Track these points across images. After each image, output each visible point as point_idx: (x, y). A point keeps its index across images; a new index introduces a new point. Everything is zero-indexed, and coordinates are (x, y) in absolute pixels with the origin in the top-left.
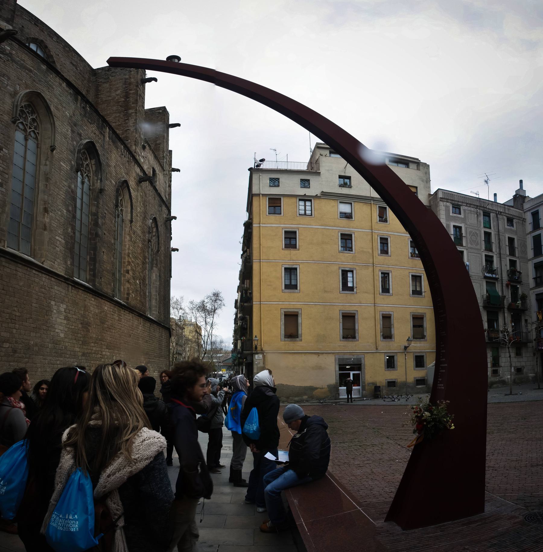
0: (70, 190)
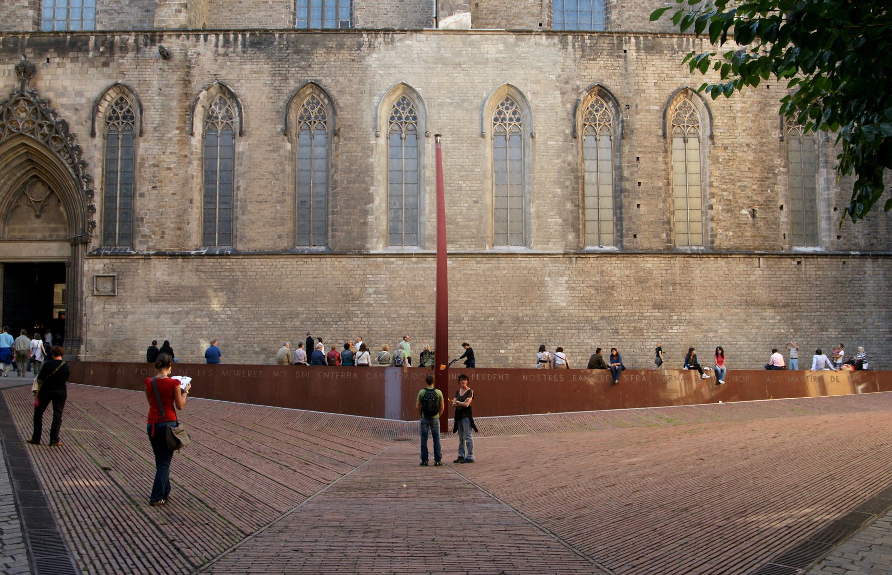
0: (566, 165)
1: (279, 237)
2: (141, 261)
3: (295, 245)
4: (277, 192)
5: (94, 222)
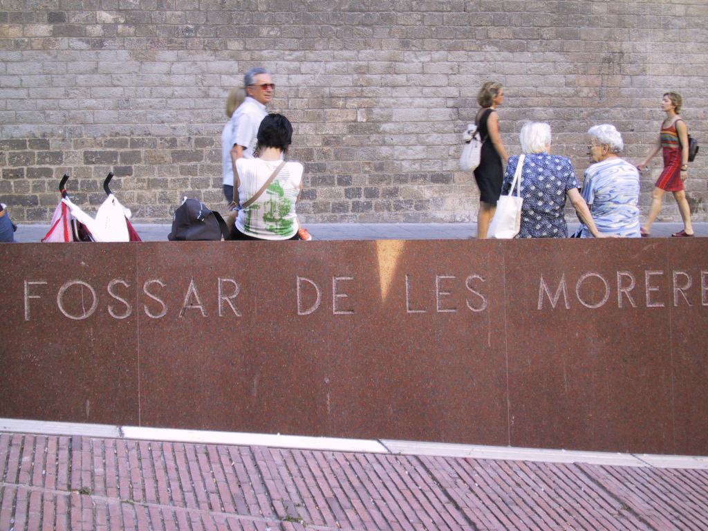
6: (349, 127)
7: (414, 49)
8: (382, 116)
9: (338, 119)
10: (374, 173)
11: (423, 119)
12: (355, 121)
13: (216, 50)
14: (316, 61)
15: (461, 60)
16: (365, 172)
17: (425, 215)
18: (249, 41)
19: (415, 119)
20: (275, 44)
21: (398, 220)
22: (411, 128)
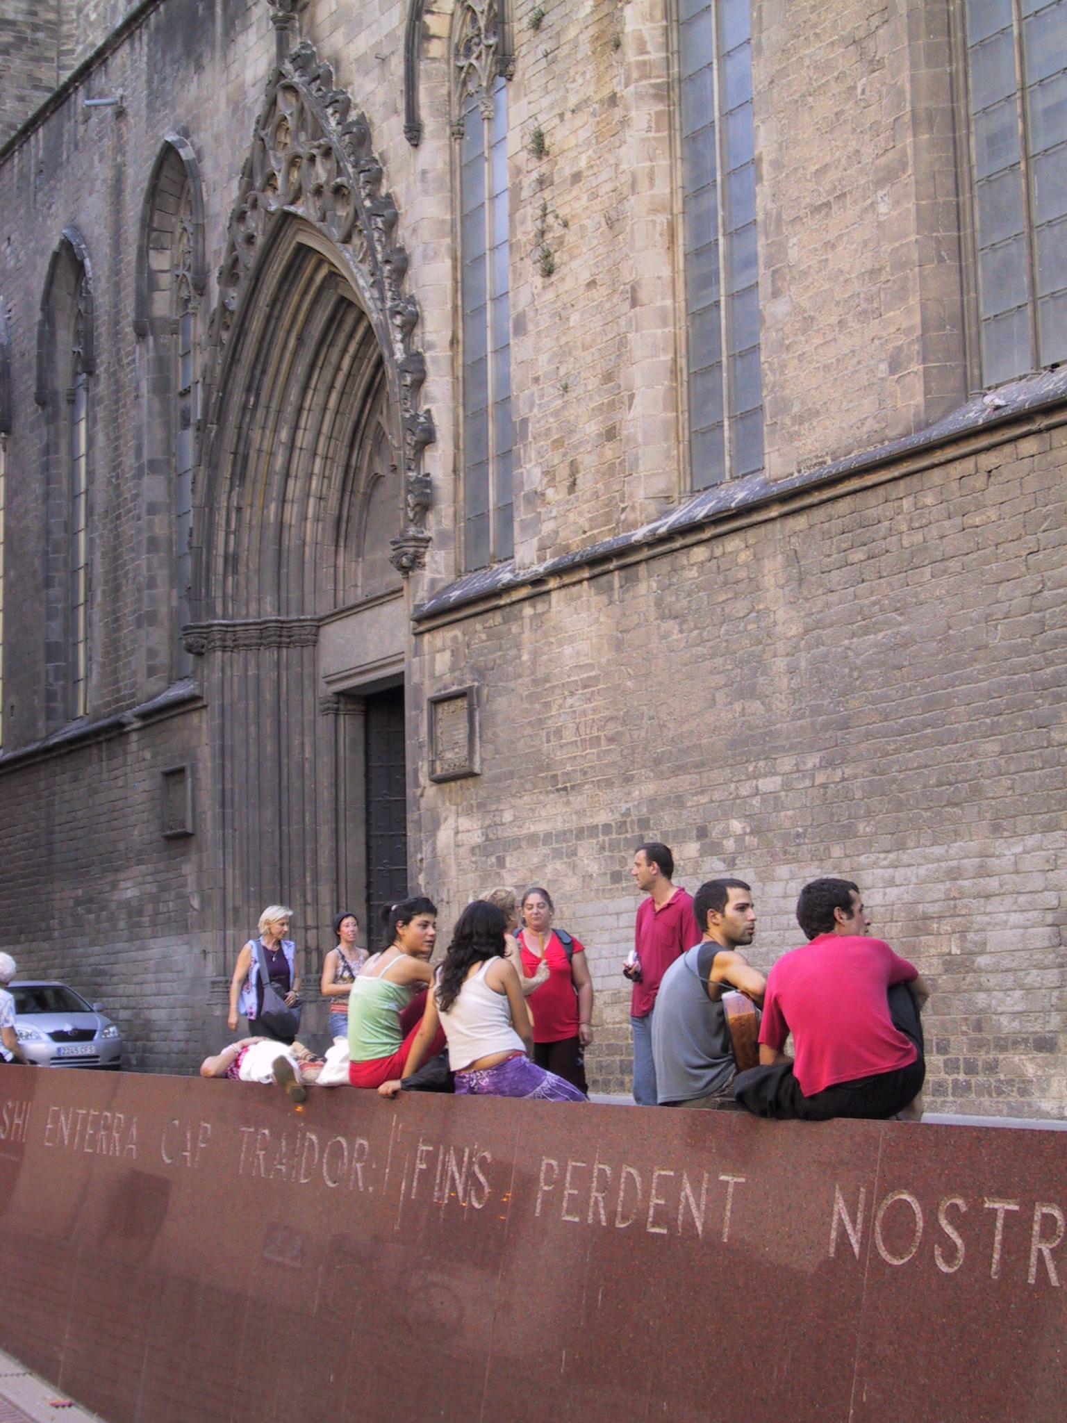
1: (894, 366)
2: (528, 610)
3: (969, 388)
4: (875, 128)
5: (426, 482)
6: (945, 963)
7: (1006, 834)
8: (975, 943)
9: (933, 951)
10: (973, 1035)
11: (1020, 946)
12: (950, 954)
13: (822, 860)
14: (909, 866)
15: (1058, 845)
16: (964, 1033)
17: (1029, 1105)
18: (849, 843)
19: (1013, 948)
20: (871, 843)
21: (999, 1112)
22: (1007, 963)
